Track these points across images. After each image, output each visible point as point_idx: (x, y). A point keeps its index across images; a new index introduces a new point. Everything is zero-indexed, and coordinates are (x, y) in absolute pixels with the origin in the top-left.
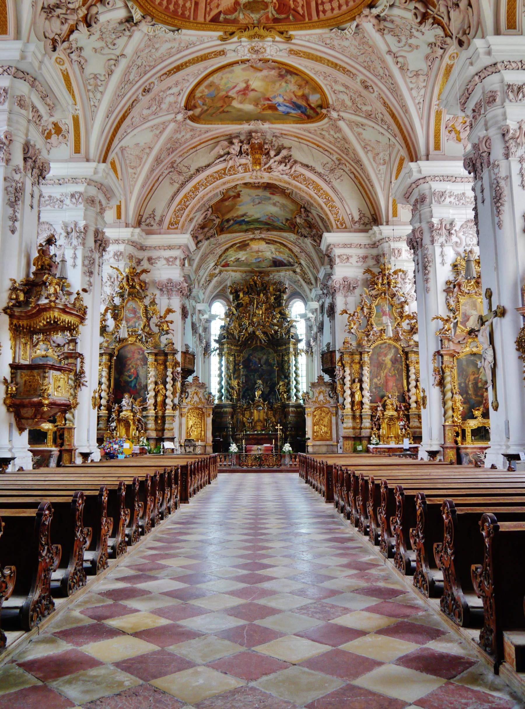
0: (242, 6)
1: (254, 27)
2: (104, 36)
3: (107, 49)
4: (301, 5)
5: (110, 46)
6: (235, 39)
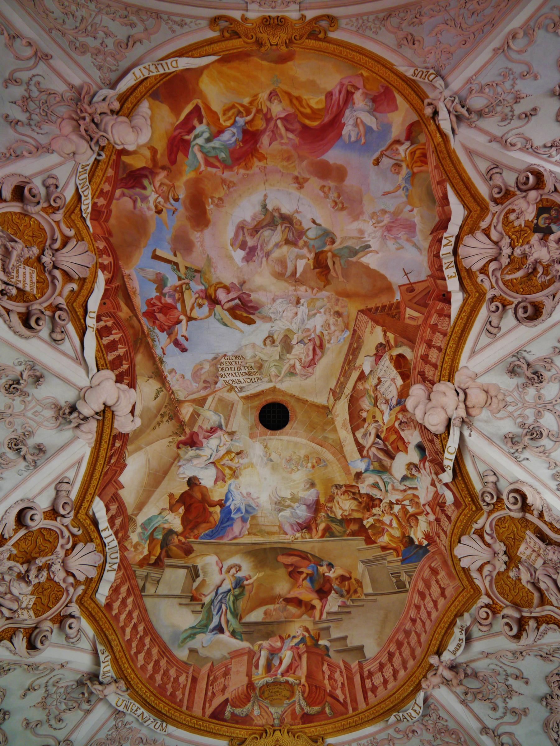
0: (257, 691)
1: (275, 731)
2: (49, 701)
3: (46, 726)
4: (340, 685)
5: (53, 722)
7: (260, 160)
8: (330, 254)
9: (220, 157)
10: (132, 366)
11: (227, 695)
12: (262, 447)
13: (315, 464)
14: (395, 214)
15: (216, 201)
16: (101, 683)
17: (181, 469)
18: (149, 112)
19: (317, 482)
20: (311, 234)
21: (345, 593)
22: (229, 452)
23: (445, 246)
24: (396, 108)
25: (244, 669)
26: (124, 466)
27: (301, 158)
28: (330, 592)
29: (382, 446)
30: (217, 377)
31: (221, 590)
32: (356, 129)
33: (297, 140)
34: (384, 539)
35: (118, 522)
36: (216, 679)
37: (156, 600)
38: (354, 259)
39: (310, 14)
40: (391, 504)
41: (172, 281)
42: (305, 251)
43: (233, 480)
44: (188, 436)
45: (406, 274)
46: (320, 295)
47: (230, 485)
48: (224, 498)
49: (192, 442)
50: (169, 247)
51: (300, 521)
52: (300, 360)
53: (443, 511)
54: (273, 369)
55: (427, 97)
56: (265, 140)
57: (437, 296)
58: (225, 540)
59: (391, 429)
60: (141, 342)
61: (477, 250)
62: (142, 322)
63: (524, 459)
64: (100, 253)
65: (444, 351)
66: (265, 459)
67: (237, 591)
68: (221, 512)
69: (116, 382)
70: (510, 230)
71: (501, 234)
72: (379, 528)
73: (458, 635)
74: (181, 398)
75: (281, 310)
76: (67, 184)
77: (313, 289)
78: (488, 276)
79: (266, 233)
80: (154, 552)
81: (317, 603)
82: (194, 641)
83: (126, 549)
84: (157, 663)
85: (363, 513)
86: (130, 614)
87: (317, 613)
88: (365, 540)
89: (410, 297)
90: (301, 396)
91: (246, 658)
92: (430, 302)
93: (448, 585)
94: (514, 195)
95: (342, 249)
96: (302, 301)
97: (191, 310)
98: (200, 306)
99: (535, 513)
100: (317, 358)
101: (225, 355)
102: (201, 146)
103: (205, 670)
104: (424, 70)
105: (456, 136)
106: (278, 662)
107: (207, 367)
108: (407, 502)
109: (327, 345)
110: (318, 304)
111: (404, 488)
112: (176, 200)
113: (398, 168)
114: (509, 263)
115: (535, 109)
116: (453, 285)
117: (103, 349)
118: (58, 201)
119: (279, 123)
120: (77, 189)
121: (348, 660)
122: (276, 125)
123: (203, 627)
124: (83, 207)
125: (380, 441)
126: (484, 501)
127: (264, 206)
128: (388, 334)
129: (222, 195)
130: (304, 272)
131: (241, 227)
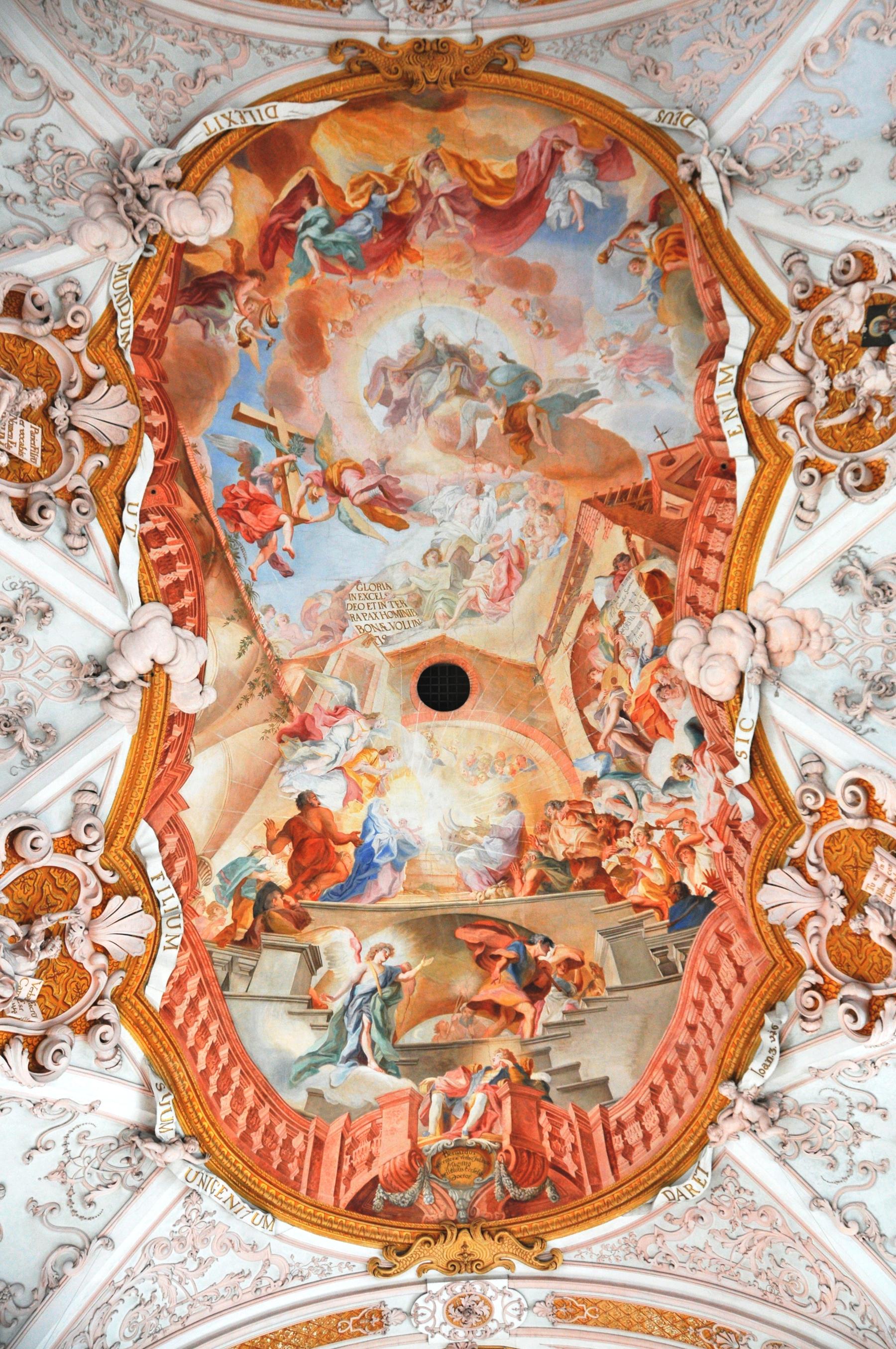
1: (459, 1230)
4: (569, 1146)
6: (410, 1275)
7: (412, 261)
8: (531, 409)
9: (346, 258)
10: (200, 598)
11: (376, 1171)
12: (425, 740)
13: (516, 767)
14: (638, 341)
15: (340, 327)
16: (158, 1141)
17: (286, 778)
18: (230, 187)
19: (519, 798)
20: (499, 377)
21: (574, 989)
22: (367, 749)
23: (721, 383)
24: (633, 172)
25: (403, 1125)
26: (187, 771)
27: (480, 256)
28: (548, 989)
29: (629, 730)
30: (345, 620)
31: (359, 990)
32: (569, 208)
33: (472, 229)
34: (638, 892)
35: (180, 865)
36: (355, 1142)
37: (249, 1004)
38: (572, 415)
39: (489, 36)
40: (648, 829)
41: (268, 457)
42: (490, 404)
43: (375, 798)
44: (296, 721)
45: (660, 436)
46: (518, 476)
47: (371, 807)
48: (360, 830)
49: (303, 733)
50: (262, 400)
51: (493, 867)
52: (486, 589)
53: (737, 834)
54: (440, 605)
55: (681, 151)
56: (420, 229)
57: (713, 468)
58: (365, 902)
59: (644, 700)
60: (214, 561)
61: (775, 386)
62: (216, 524)
64: (146, 407)
65: (727, 560)
66: (430, 760)
67: (388, 992)
68: (356, 853)
69: (173, 624)
70: (824, 351)
71: (811, 357)
72: (628, 873)
74: (285, 656)
75: (450, 504)
76: (94, 293)
77: (505, 468)
78: (793, 427)
79: (424, 377)
80: (243, 922)
81: (525, 1008)
82: (316, 1077)
83: (195, 913)
84: (253, 1112)
85: (601, 848)
86: (204, 1026)
87: (526, 1026)
88: (606, 895)
89: (667, 474)
90: (489, 651)
91: (406, 1106)
92: (702, 479)
93: (749, 960)
94: (829, 293)
95: (553, 398)
96: (486, 488)
97: (299, 506)
98: (314, 499)
100: (514, 584)
101: (358, 583)
102: (314, 240)
103: (336, 1127)
104: (675, 112)
105: (731, 210)
106: (462, 1112)
107: (327, 602)
108: (675, 824)
109: (532, 562)
110: (514, 492)
111: (670, 799)
112: (274, 325)
113: (638, 265)
114: (827, 405)
115: (854, 162)
116: (737, 446)
117: (155, 568)
118: (79, 318)
119: (442, 202)
120: (111, 302)
121: (579, 1104)
122: (437, 206)
123: (330, 1054)
124: (120, 332)
125: (626, 722)
127: (420, 335)
128: (634, 538)
129: (349, 317)
130: (489, 438)
131: (382, 369)
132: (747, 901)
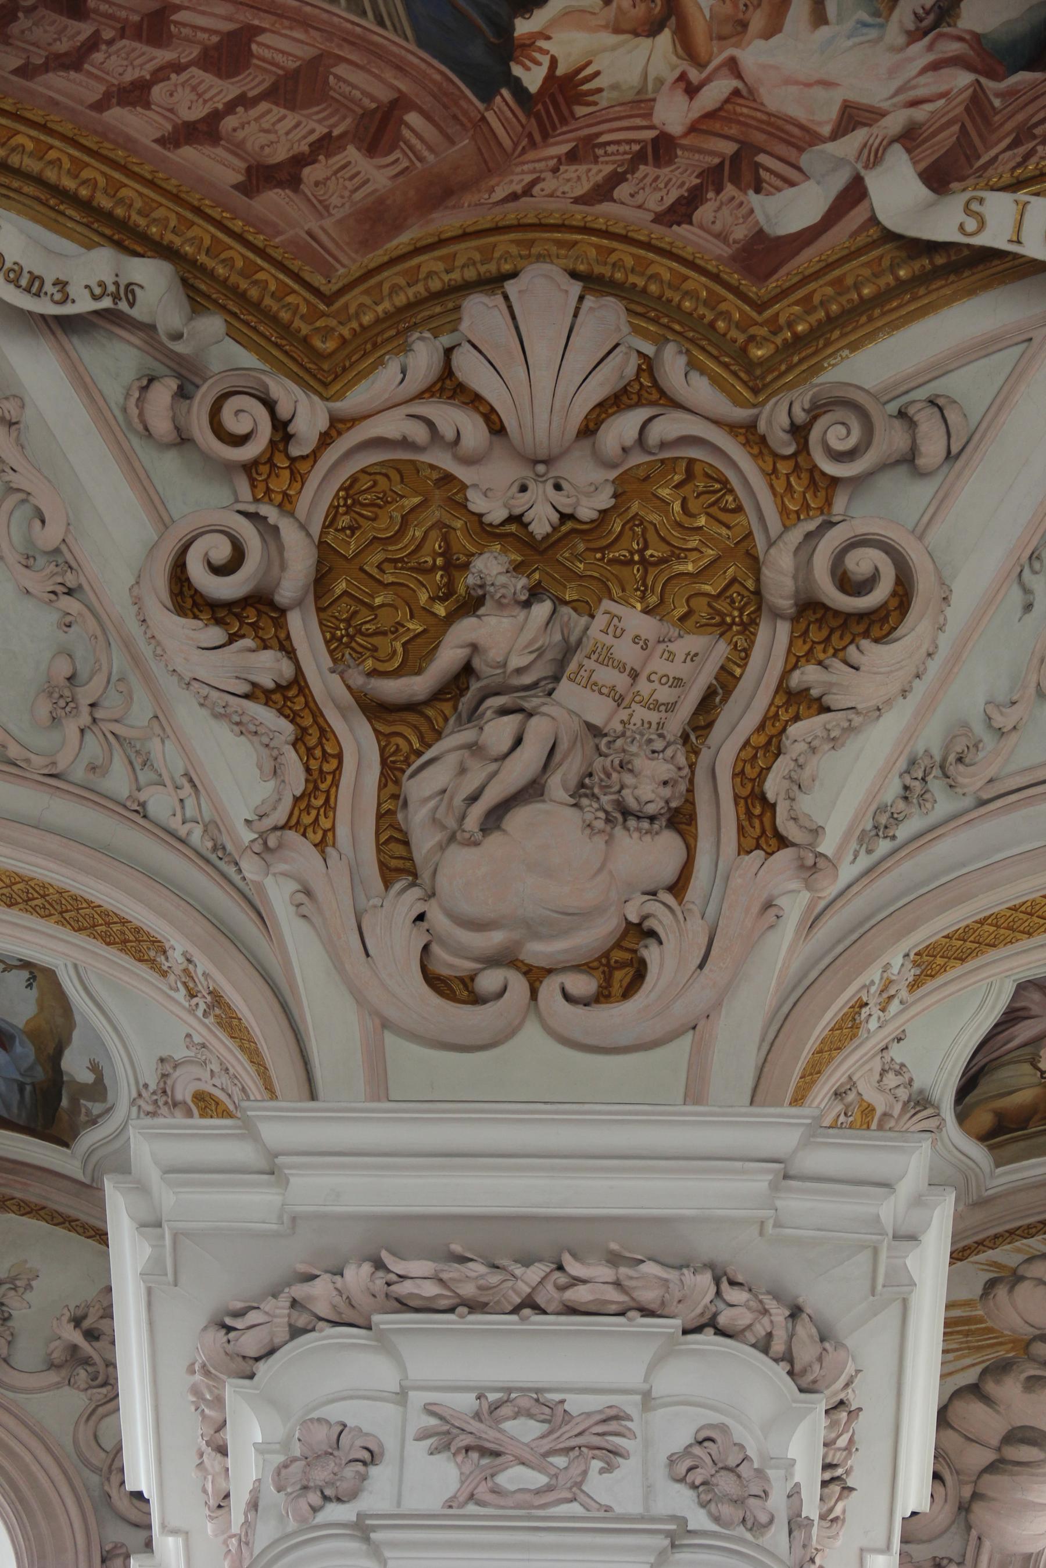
53: (713, 178)
63: (1026, 591)
73: (89, 270)
93: (321, 209)
99: (809, 675)
126: (816, 410)
132: (511, 213)
